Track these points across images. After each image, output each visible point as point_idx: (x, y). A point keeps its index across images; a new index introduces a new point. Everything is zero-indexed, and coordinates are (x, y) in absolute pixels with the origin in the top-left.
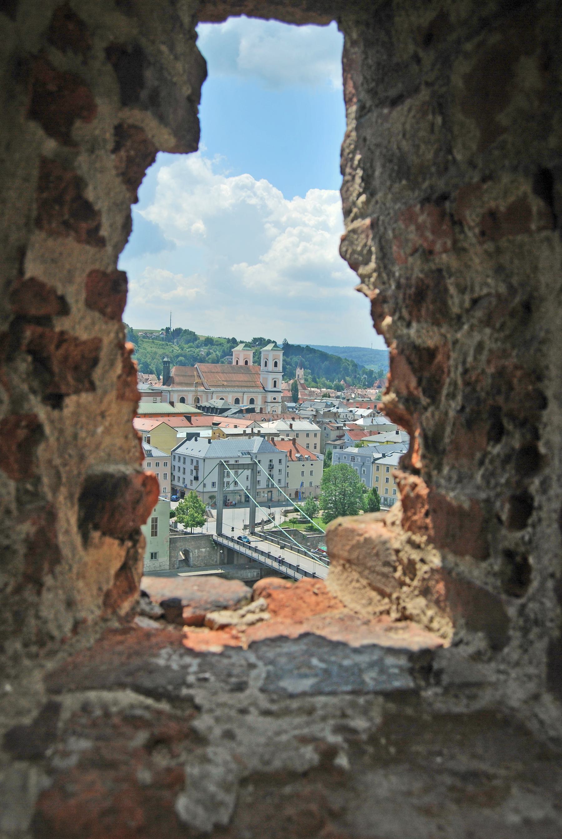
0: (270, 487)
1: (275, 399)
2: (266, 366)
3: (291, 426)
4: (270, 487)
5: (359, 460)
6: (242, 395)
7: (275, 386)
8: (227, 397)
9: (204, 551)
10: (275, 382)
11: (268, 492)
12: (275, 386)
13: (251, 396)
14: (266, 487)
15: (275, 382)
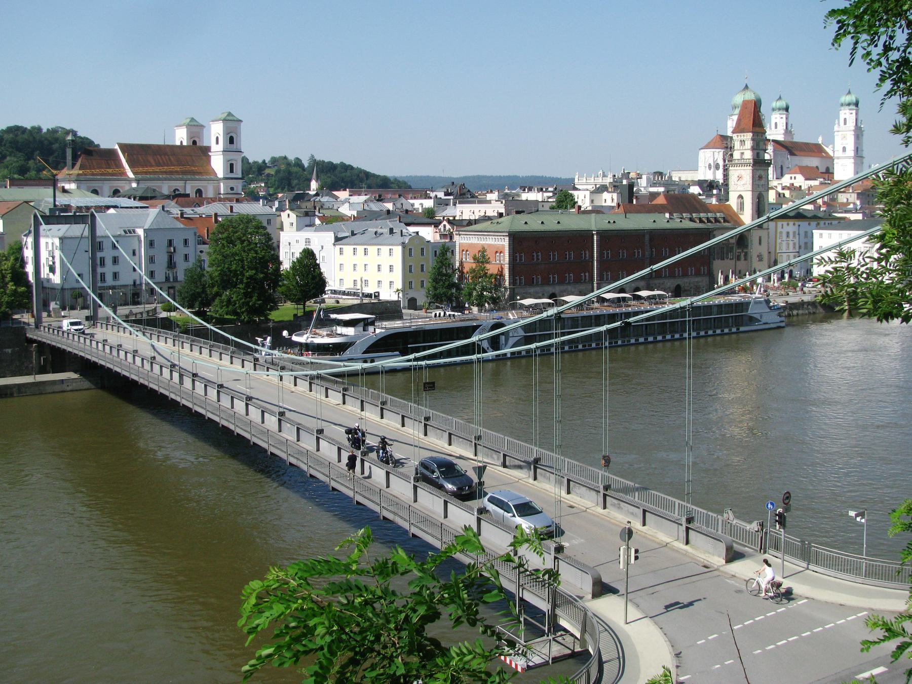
0: (171, 280)
1: (232, 189)
2: (217, 143)
3: (232, 208)
4: (171, 280)
5: (316, 243)
6: (184, 184)
7: (232, 171)
8: (160, 187)
9: (10, 352)
10: (232, 166)
11: (169, 288)
12: (232, 171)
13: (197, 186)
14: (164, 280)
15: (232, 166)
